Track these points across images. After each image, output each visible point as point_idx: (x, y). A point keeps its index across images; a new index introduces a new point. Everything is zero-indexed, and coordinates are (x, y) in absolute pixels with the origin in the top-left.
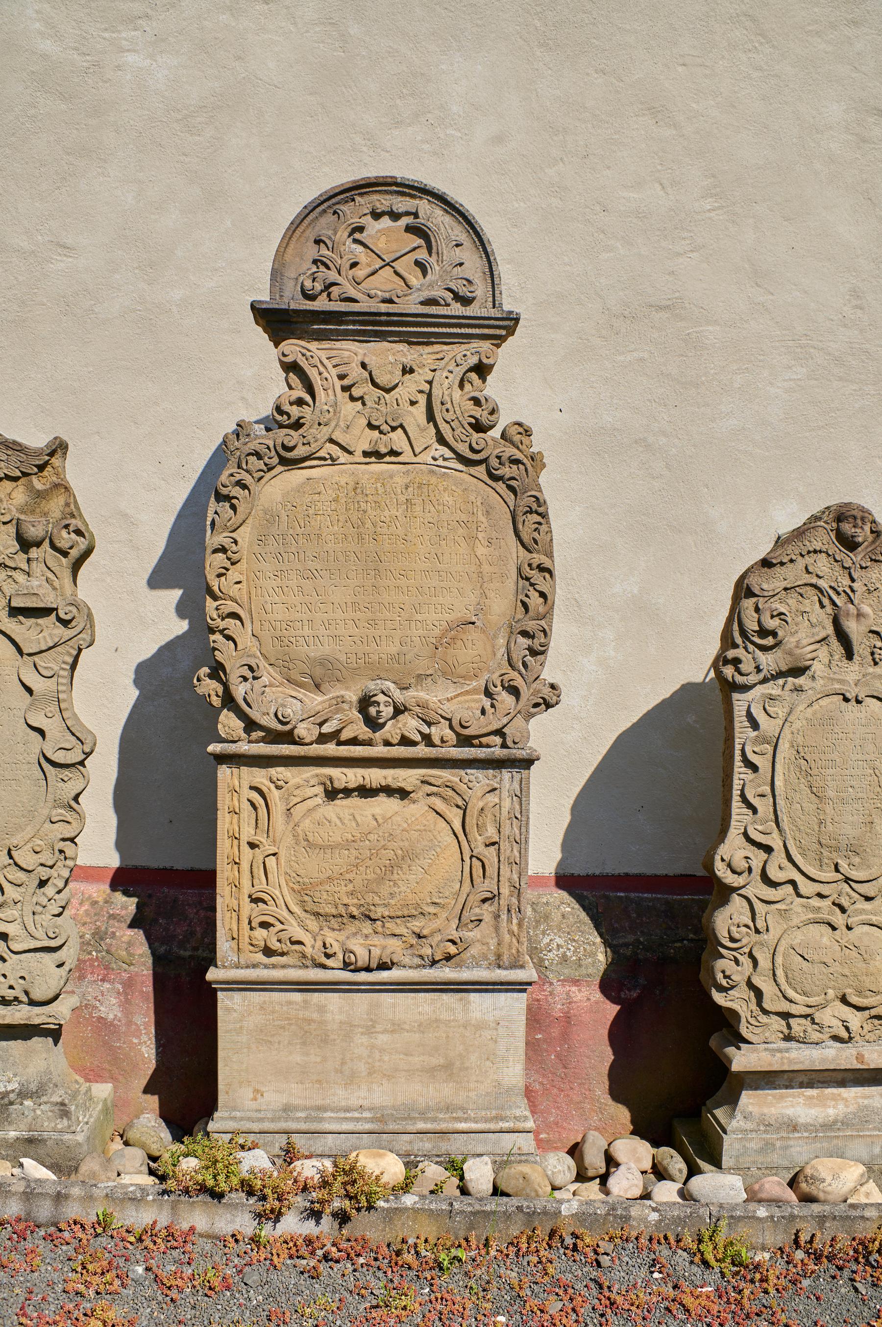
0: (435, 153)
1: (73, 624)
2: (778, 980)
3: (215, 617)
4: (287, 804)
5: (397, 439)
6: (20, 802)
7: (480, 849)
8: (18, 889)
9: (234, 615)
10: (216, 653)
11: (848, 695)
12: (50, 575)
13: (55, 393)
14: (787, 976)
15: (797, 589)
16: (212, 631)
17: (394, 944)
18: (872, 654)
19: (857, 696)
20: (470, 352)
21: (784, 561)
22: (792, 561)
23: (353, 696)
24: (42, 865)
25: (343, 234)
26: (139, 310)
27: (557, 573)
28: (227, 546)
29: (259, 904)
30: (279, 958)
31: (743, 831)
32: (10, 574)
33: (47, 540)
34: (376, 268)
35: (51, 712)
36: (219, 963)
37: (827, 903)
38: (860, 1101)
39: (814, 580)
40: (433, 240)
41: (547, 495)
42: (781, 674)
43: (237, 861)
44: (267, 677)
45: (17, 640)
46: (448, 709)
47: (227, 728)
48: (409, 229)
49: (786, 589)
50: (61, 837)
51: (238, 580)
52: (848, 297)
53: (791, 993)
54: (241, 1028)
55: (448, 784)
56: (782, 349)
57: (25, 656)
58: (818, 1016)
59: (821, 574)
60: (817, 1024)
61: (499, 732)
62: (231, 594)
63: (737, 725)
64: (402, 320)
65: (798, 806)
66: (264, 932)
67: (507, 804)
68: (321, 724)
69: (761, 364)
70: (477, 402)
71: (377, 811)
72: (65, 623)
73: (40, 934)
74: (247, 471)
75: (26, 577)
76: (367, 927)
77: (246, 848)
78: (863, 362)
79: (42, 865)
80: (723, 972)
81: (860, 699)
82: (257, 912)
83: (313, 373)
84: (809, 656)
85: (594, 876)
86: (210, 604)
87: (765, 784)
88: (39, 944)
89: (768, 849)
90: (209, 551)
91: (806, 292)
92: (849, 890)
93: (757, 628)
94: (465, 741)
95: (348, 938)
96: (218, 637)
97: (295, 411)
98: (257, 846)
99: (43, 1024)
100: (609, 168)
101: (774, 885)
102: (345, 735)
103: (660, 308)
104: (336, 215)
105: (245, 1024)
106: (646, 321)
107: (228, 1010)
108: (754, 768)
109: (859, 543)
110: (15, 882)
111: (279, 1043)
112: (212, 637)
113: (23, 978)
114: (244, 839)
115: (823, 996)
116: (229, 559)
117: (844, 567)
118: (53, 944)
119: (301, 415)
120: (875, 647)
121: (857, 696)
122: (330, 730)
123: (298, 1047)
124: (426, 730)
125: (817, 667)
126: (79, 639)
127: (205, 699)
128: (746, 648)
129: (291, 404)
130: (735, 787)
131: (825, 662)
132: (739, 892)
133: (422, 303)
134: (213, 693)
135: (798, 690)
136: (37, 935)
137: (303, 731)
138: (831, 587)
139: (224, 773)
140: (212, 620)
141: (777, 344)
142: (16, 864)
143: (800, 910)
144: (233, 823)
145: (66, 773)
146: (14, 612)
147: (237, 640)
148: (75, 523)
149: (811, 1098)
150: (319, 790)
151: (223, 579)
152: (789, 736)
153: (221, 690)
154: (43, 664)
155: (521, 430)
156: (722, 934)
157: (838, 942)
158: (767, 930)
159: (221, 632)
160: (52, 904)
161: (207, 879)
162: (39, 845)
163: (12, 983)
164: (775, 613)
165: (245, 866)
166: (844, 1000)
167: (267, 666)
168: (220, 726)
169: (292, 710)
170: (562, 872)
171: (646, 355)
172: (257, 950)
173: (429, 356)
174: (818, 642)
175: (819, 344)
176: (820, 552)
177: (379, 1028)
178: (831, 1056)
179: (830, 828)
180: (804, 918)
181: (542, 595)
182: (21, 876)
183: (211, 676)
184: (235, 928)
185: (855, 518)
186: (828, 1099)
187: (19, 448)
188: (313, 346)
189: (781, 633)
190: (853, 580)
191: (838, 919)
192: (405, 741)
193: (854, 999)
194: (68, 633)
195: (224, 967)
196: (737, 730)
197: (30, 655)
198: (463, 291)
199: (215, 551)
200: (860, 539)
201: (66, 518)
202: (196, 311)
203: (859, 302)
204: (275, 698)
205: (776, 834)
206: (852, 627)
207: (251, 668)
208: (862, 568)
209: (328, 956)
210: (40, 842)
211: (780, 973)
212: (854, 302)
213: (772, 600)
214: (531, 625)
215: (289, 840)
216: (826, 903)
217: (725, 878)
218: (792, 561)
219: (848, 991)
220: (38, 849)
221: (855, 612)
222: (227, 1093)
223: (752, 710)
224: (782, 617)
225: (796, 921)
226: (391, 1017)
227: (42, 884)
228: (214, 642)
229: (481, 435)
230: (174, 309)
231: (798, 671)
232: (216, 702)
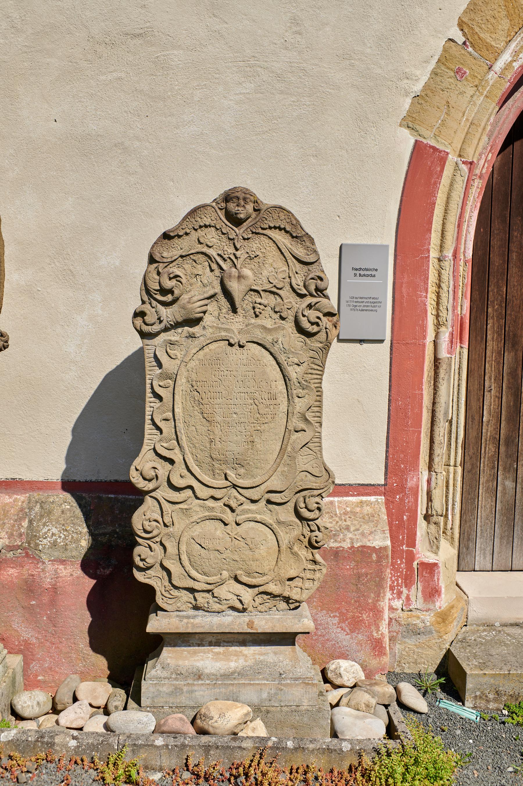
2: (183, 562)
11: (232, 341)
14: (190, 560)
15: (191, 256)
18: (254, 308)
19: (239, 342)
21: (180, 234)
22: (187, 234)
31: (153, 447)
37: (220, 504)
38: (257, 657)
39: (205, 250)
42: (178, 325)
49: (182, 256)
52: (288, 25)
53: (194, 573)
56: (234, 69)
58: (216, 591)
59: (210, 244)
60: (216, 597)
63: (147, 364)
65: (194, 428)
69: (217, 81)
78: (300, 78)
80: (140, 556)
81: (241, 343)
84: (199, 310)
87: (168, 411)
89: (171, 462)
92: (237, 494)
93: (158, 288)
101: (177, 489)
103: (135, 36)
106: (123, 47)
108: (159, 398)
109: (241, 219)
115: (219, 576)
117: (229, 239)
120: (255, 303)
121: (239, 342)
125: (208, 319)
128: (150, 303)
130: (147, 413)
131: (215, 315)
135: (192, 336)
138: (218, 255)
141: (230, 64)
143: (198, 509)
149: (219, 653)
152: (185, 374)
157: (229, 534)
158: (173, 524)
164: (171, 276)
166: (236, 579)
170: (66, 479)
171: (123, 75)
174: (208, 298)
175: (265, 64)
176: (210, 226)
178: (231, 622)
179: (219, 445)
180: (201, 515)
185: (238, 198)
186: (231, 655)
189: (177, 292)
190: (237, 249)
191: (229, 517)
193: (244, 579)
196: (147, 369)
200: (242, 216)
203: (298, 29)
205: (177, 450)
206: (234, 286)
208: (244, 239)
211: (184, 557)
212: (295, 29)
213: (171, 265)
216: (219, 504)
217: (138, 483)
218: (187, 234)
219: (239, 572)
221: (237, 275)
223: (157, 353)
224: (178, 278)
225: (195, 518)
231: (194, 322)
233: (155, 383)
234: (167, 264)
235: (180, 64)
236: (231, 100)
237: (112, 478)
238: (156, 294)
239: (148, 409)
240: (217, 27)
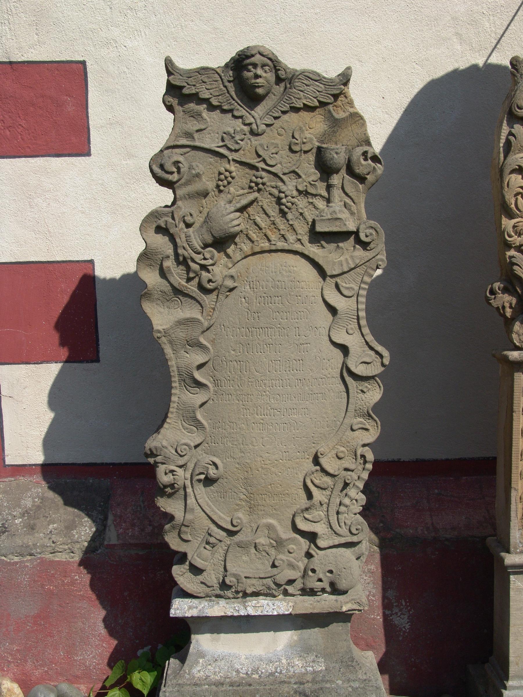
1: (372, 246)
3: (513, 234)
6: (326, 413)
8: (324, 492)
10: (515, 267)
12: (348, 201)
13: (285, 35)
24: (346, 470)
32: (311, 200)
33: (345, 167)
35: (352, 329)
36: (512, 549)
45: (321, 262)
57: (328, 278)
72: (365, 245)
75: (325, 203)
79: (346, 470)
86: (507, 224)
88: (343, 540)
90: (507, 170)
99: (349, 610)
110: (322, 486)
113: (331, 572)
118: (355, 539)
126: (378, 260)
127: (500, 311)
134: (507, 305)
140: (510, 236)
142: (323, 470)
145: (365, 385)
146: (317, 236)
154: (344, 285)
160: (353, 504)
162: (342, 452)
163: (321, 576)
168: (514, 336)
182: (328, 480)
183: (505, 290)
187: (318, 78)
194: (368, 255)
195: (516, 553)
197: (332, 276)
201: (361, 145)
210: (342, 449)
220: (341, 455)
222: (517, 664)
228: (511, 257)
232: (509, 312)
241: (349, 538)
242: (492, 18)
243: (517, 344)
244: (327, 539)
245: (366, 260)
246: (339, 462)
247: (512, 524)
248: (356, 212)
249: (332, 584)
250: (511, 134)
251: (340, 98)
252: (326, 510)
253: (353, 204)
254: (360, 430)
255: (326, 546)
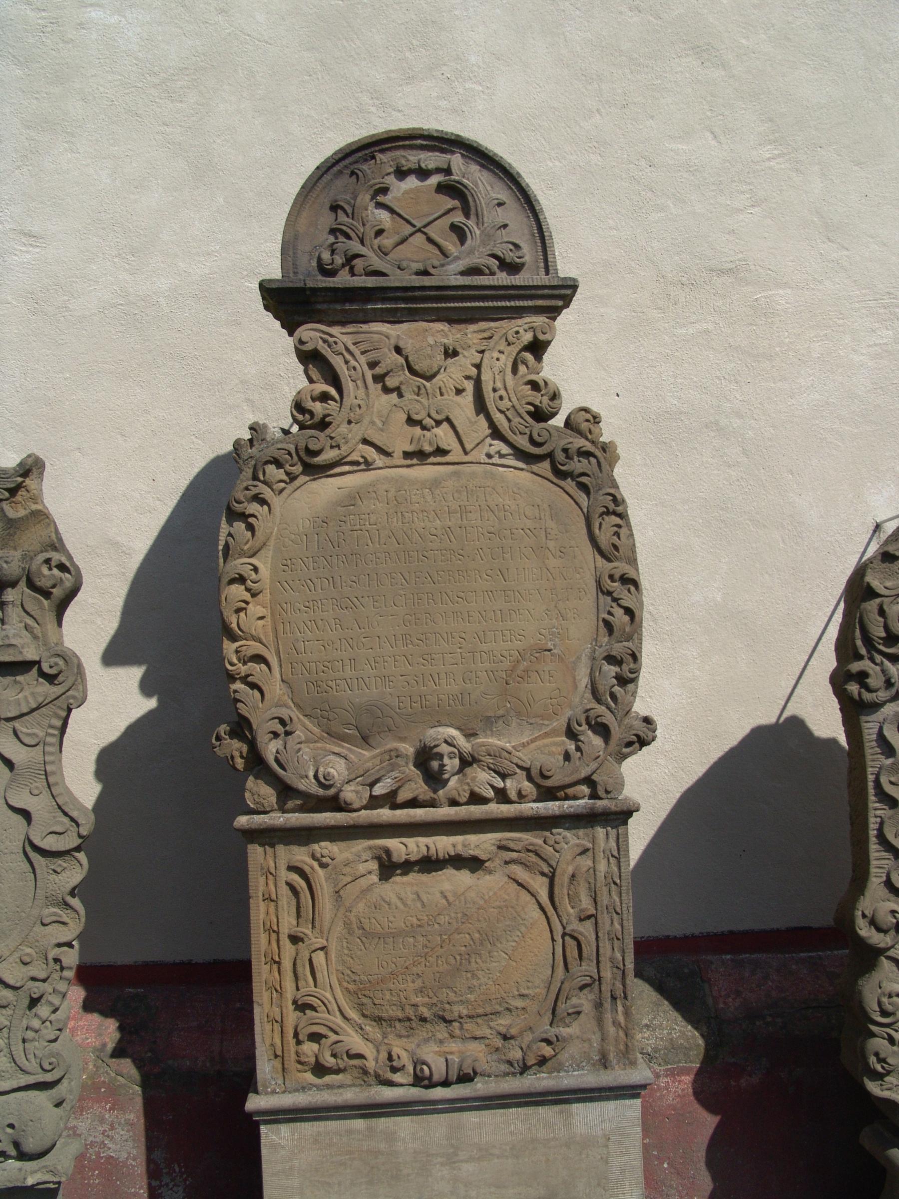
0: (454, 111)
1: (61, 678)
3: (235, 661)
4: (335, 887)
5: (443, 435)
7: (574, 926)
9: (259, 659)
10: (239, 705)
12: (30, 621)
16: (232, 678)
17: (476, 1050)
20: (523, 329)
23: (409, 749)
24: (33, 979)
25: (365, 198)
26: (121, 305)
27: (644, 582)
28: (246, 575)
29: (307, 1012)
30: (333, 1076)
31: (884, 878)
33: (24, 579)
34: (401, 237)
35: (37, 788)
36: (260, 1088)
40: (470, 199)
41: (626, 491)
43: (277, 959)
44: (301, 731)
46: (525, 757)
47: (256, 796)
48: (441, 188)
50: (55, 941)
51: (261, 615)
54: (291, 1168)
55: (530, 848)
56: (863, 311)
61: (589, 781)
62: (254, 633)
63: (868, 752)
64: (442, 292)
66: (315, 1047)
67: (602, 867)
68: (372, 785)
70: (535, 386)
71: (446, 886)
72: (51, 679)
73: (32, 1065)
74: (265, 483)
76: (441, 1031)
77: (286, 943)
79: (33, 979)
80: (877, 1054)
82: (307, 1023)
83: (337, 362)
85: (693, 937)
86: (229, 648)
88: (31, 1080)
90: (225, 580)
91: (885, 245)
93: (883, 635)
94: (548, 794)
95: (418, 1045)
96: (238, 686)
97: (318, 408)
98: (302, 940)
100: (652, 117)
102: (403, 796)
103: (722, 272)
104: (354, 177)
105: (296, 1163)
106: (707, 288)
107: (274, 1147)
111: (339, 1184)
112: (233, 687)
114: (285, 931)
116: (248, 590)
118: (49, 1077)
119: (327, 412)
122: (384, 792)
123: (364, 1187)
124: (500, 784)
129: (314, 400)
130: (872, 826)
132: (889, 953)
133: (462, 273)
134: (236, 754)
136: (30, 1069)
137: (350, 794)
139: (256, 853)
140: (232, 664)
141: (857, 305)
144: (270, 912)
147: (264, 688)
148: (56, 557)
150: (374, 866)
151: (242, 614)
153: (245, 749)
154: (25, 730)
155: (589, 416)
156: (872, 1006)
159: (244, 680)
160: (46, 1027)
161: (234, 976)
162: (28, 954)
165: (287, 964)
167: (301, 717)
169: (337, 770)
171: (711, 327)
172: (307, 1068)
173: (475, 335)
177: (462, 1155)
181: (629, 611)
183: (233, 734)
184: (278, 1041)
188: (335, 330)
192: (476, 799)
194: (56, 690)
195: (267, 1093)
196: (869, 757)
198: (511, 256)
199: (232, 581)
201: (46, 551)
202: (188, 302)
204: (320, 760)
207: (282, 722)
209: (394, 1070)
210: (29, 950)
214: (618, 649)
215: (339, 928)
217: (870, 937)
226: (476, 1140)
227: (34, 1002)
228: (235, 691)
229: (542, 425)
230: (162, 300)
232: (240, 763)
233: (884, 780)
234: (892, 598)
235: (789, 308)
236: (864, 354)
237: (724, 927)
238: (879, 644)
239: (872, 820)
240: (835, 255)
241: (40, 1076)
242: (292, 381)
243: (252, 806)
244: (9, 1078)
245: (53, 698)
246: (24, 969)
247: (258, 1053)
248: (40, 635)
249: (16, 1145)
250: (230, 535)
251: (20, 493)
252: (7, 1036)
253: (36, 625)
254: (56, 924)
255: (7, 1089)
